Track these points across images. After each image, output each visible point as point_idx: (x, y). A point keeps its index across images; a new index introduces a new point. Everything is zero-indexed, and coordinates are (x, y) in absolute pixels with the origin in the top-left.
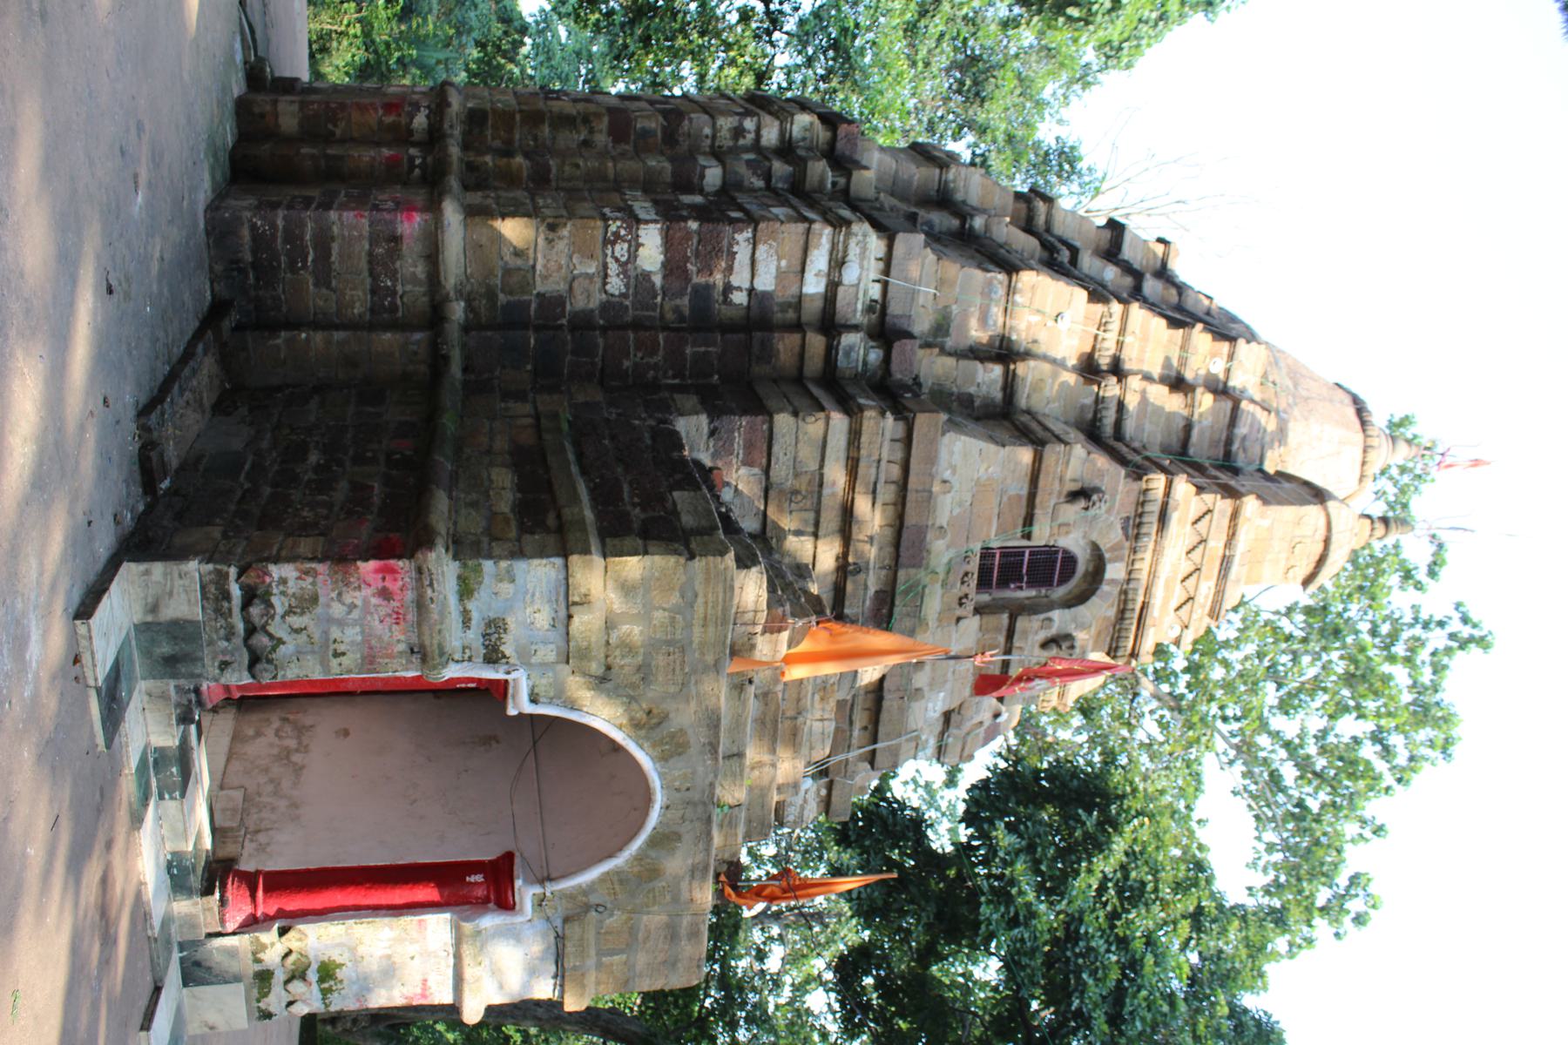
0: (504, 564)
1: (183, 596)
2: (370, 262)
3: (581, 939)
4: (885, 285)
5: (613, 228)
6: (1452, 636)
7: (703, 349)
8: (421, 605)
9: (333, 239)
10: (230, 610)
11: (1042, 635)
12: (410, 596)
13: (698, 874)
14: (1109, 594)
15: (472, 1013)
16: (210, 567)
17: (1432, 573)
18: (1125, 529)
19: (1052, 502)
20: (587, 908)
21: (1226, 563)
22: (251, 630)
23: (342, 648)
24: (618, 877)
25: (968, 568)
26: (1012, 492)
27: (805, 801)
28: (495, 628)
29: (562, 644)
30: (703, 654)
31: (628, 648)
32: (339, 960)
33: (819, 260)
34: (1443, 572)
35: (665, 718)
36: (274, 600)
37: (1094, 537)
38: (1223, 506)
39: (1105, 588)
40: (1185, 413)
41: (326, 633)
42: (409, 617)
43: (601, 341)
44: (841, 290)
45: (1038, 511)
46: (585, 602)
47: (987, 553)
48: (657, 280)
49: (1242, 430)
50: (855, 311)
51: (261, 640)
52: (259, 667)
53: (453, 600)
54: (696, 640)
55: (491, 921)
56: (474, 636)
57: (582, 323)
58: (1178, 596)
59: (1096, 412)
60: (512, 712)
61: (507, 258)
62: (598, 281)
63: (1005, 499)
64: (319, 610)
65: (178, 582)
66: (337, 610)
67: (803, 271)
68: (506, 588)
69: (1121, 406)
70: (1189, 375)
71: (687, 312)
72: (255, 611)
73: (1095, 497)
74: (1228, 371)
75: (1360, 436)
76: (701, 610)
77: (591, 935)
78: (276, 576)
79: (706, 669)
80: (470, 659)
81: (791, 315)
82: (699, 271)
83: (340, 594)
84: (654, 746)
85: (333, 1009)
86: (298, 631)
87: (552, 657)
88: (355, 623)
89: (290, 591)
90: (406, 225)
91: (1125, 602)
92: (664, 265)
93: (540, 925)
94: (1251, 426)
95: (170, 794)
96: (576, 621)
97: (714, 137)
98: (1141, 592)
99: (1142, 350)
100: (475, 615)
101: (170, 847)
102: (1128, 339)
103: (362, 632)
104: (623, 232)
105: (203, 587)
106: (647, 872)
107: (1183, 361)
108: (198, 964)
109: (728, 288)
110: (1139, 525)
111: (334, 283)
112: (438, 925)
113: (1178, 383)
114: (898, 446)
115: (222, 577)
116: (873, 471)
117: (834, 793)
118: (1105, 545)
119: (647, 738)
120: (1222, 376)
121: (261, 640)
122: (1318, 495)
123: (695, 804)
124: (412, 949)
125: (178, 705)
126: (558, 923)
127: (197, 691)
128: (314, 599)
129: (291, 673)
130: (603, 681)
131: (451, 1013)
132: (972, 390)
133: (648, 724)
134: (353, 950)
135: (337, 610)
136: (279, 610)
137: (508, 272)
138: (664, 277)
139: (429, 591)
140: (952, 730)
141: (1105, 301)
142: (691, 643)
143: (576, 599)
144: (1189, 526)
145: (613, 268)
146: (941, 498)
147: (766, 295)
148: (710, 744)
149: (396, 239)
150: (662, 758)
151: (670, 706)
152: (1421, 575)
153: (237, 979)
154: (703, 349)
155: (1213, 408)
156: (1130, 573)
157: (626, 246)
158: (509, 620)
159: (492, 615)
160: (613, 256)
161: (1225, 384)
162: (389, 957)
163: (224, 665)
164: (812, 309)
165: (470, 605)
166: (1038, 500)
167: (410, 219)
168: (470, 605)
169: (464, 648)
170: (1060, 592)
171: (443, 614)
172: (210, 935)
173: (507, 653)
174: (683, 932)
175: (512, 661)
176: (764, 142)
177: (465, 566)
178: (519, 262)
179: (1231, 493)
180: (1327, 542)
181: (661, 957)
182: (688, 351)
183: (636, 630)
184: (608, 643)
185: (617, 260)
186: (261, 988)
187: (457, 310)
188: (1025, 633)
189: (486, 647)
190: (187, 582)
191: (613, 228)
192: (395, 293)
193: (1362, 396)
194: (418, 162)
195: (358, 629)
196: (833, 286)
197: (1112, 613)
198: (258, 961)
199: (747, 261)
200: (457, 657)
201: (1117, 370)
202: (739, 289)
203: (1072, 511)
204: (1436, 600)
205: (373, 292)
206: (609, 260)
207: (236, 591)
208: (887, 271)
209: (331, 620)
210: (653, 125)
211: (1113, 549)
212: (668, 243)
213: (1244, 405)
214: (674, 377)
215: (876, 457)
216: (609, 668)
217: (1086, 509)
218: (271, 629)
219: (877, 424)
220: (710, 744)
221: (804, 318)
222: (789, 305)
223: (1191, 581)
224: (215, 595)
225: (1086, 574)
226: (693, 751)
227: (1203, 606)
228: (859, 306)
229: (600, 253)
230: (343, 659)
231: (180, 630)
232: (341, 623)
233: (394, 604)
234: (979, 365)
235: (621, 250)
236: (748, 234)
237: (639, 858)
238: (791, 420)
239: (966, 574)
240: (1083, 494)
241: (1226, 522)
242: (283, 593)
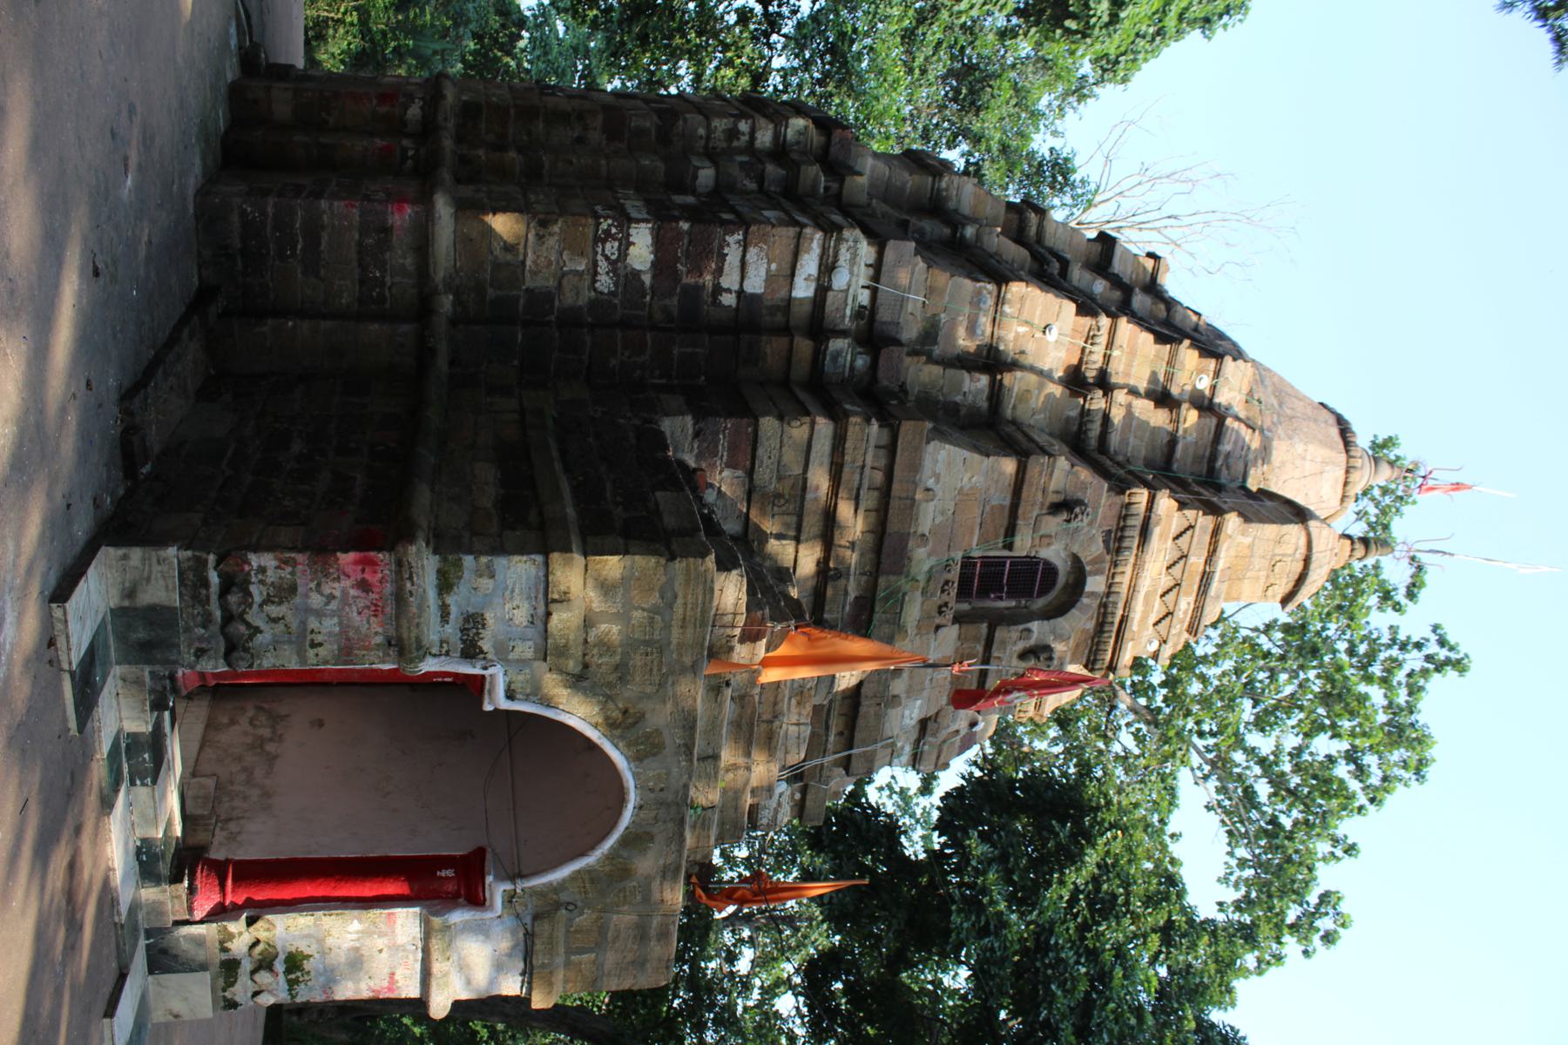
0: (484, 559)
1: (161, 582)
2: (359, 252)
3: (551, 937)
4: (874, 292)
5: (604, 226)
6: (1429, 658)
7: (690, 350)
8: (400, 598)
9: (323, 227)
10: (208, 597)
11: (1021, 646)
12: (388, 588)
13: (669, 874)
14: (1088, 606)
15: (439, 1007)
16: (189, 553)
17: (1411, 595)
18: (1106, 542)
20: (558, 905)
21: (1206, 579)
22: (228, 618)
23: (319, 638)
24: (588, 875)
25: (949, 576)
27: (779, 804)
28: (473, 622)
29: (540, 641)
30: (680, 655)
31: (605, 646)
32: (307, 951)
33: (809, 265)
34: (1423, 594)
35: (641, 717)
36: (253, 588)
37: (1075, 549)
38: (1205, 522)
39: (1085, 600)
40: (1170, 428)
41: (303, 623)
42: (388, 609)
43: (588, 339)
44: (830, 294)
45: (1020, 522)
46: (564, 599)
47: (968, 563)
48: (647, 279)
49: (1226, 447)
50: (844, 316)
52: (235, 655)
53: (432, 594)
54: (674, 641)
55: (458, 917)
56: (451, 630)
57: (571, 320)
58: (1157, 610)
59: (1081, 425)
60: (488, 707)
61: (497, 252)
62: (587, 278)
63: (988, 508)
64: (298, 600)
65: (156, 568)
66: (316, 600)
67: (793, 275)
68: (486, 584)
69: (1106, 418)
70: (1175, 391)
71: (675, 314)
72: (233, 599)
73: (1077, 510)
74: (1214, 388)
75: (1344, 455)
76: (681, 611)
77: (560, 934)
78: (255, 565)
79: (683, 671)
80: (447, 654)
81: (779, 318)
82: (689, 272)
83: (319, 585)
84: (629, 745)
85: (299, 1000)
86: (275, 620)
87: (529, 654)
88: (333, 614)
89: (269, 580)
90: (397, 217)
91: (1105, 614)
92: (654, 264)
93: (509, 921)
94: (1236, 443)
95: (142, 780)
96: (555, 619)
97: (708, 138)
98: (1121, 605)
99: (1129, 365)
100: (454, 610)
101: (140, 833)
102: (1116, 353)
103: (340, 624)
104: (614, 230)
105: (181, 574)
106: (617, 872)
107: (1170, 377)
108: (164, 952)
109: (718, 290)
110: (1121, 539)
111: (322, 272)
112: (406, 922)
113: (1162, 398)
114: (882, 452)
115: (201, 565)
116: (857, 477)
117: (809, 797)
118: (1086, 557)
119: (622, 737)
120: (1207, 392)
122: (1299, 514)
123: (668, 805)
124: (380, 942)
125: (152, 691)
126: (528, 920)
127: (172, 677)
128: (293, 589)
129: (268, 662)
130: (580, 680)
131: (418, 1007)
132: (958, 398)
133: (622, 724)
134: (321, 941)
136: (257, 599)
137: (497, 266)
138: (654, 277)
139: (408, 585)
140: (929, 739)
141: (1094, 315)
142: (669, 643)
143: (556, 596)
145: (603, 266)
146: (924, 505)
147: (753, 296)
148: (686, 745)
149: (386, 230)
150: (637, 758)
151: (646, 706)
152: (1400, 596)
153: (203, 967)
154: (690, 350)
155: (1198, 423)
156: (1110, 586)
157: (616, 244)
158: (489, 616)
159: (471, 610)
160: (604, 254)
161: (1211, 400)
162: (357, 949)
163: (200, 653)
164: (801, 313)
165: (450, 600)
166: (1020, 511)
167: (400, 210)
168: (450, 600)
169: (442, 642)
170: (1040, 603)
171: (422, 607)
172: (178, 923)
173: (485, 648)
174: (653, 932)
175: (489, 656)
176: (758, 144)
177: (444, 560)
178: (509, 257)
179: (1215, 510)
180: (1307, 561)
181: (630, 957)
182: (676, 351)
183: (615, 629)
184: (586, 641)
185: (607, 258)
186: (226, 978)
187: (446, 303)
188: (1003, 643)
189: (464, 642)
190: (165, 568)
191: (604, 226)
192: (383, 284)
193: (1347, 416)
194: (410, 153)
195: (336, 620)
197: (1091, 625)
198: (225, 950)
199: (737, 263)
200: (434, 651)
201: (1104, 383)
202: (729, 291)
203: (1053, 524)
204: (1414, 623)
205: (362, 282)
206: (599, 257)
207: (214, 578)
208: (876, 277)
209: (308, 610)
210: (648, 124)
211: (1094, 561)
212: (659, 243)
213: (1229, 421)
214: (660, 377)
215: (860, 463)
216: (586, 666)
217: (1068, 521)
218: (248, 618)
219: (863, 430)
220: (686, 745)
221: (792, 323)
222: (778, 308)
223: (1171, 596)
224: (193, 581)
225: (1067, 585)
226: (669, 751)
227: (1182, 622)
228: (848, 312)
229: (589, 250)
230: (321, 650)
231: (158, 616)
232: (319, 614)
233: (372, 596)
234: (966, 375)
235: (611, 248)
236: (739, 236)
237: (611, 857)
238: (776, 423)
239: (947, 582)
240: (1066, 506)
241: (1208, 538)
242: (262, 582)
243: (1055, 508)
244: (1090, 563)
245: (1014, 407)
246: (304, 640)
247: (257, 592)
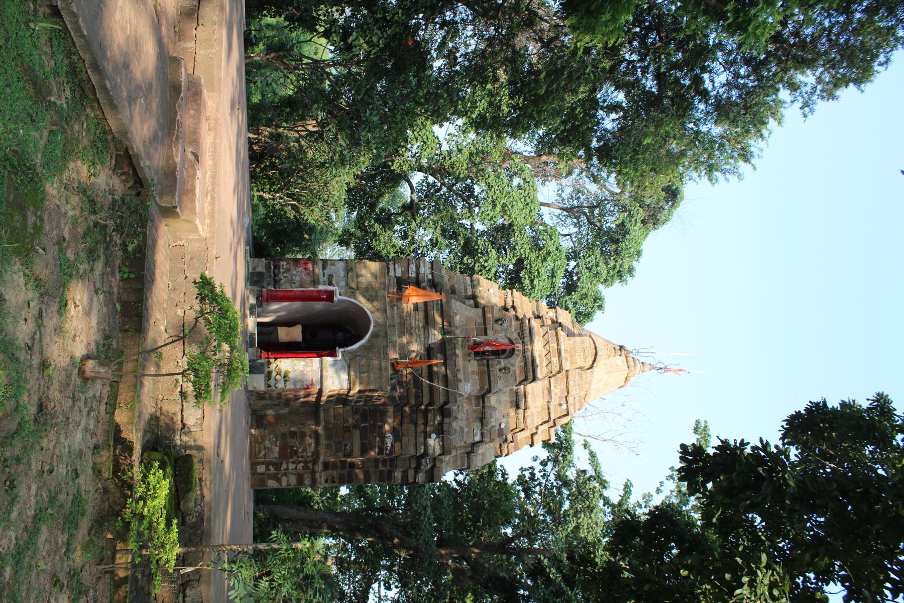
4: (432, 274)
11: (498, 367)
22: (275, 275)
24: (363, 347)
28: (331, 276)
33: (413, 268)
51: (277, 278)
56: (326, 279)
58: (545, 363)
66: (295, 272)
107: (538, 311)
118: (513, 338)
121: (277, 278)
124: (309, 369)
129: (283, 288)
135: (295, 272)
180: (596, 348)
181: (377, 376)
196: (418, 274)
197: (522, 364)
201: (514, 307)
203: (497, 326)
223: (548, 356)
224: (268, 267)
231: (260, 275)
237: (369, 340)
243: (497, 321)
246: (292, 282)
247: (282, 271)
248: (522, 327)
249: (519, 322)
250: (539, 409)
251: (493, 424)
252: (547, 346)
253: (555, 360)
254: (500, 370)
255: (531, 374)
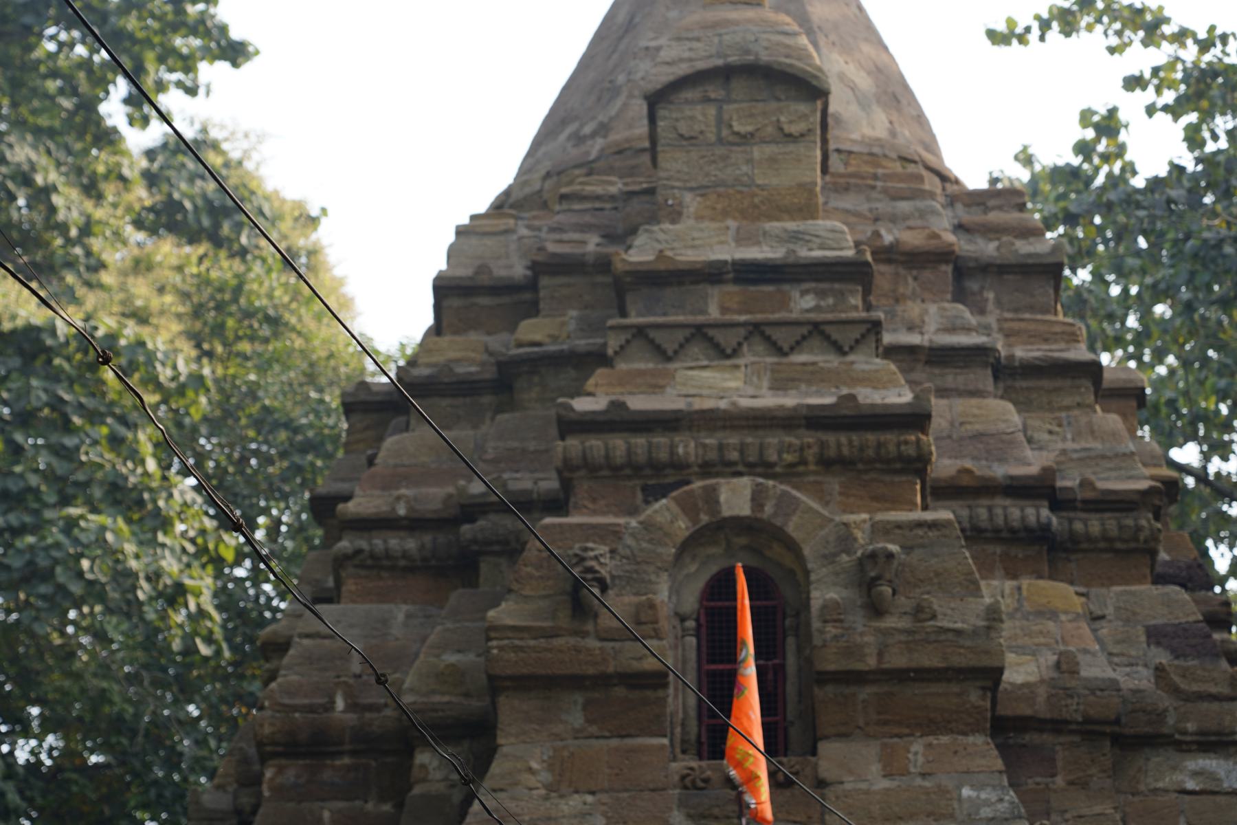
11: (858, 620)
19: (592, 643)
21: (750, 273)
26: (577, 718)
63: (593, 729)
110: (657, 467)
118: (683, 527)
144: (672, 366)
166: (591, 671)
211: (689, 508)
223: (782, 337)
234: (417, 790)
244: (695, 520)
245: (467, 695)
248: (612, 472)
249: (583, 488)
250: (1040, 425)
251: (1143, 679)
252: (727, 339)
253: (803, 303)
254: (876, 609)
255: (890, 438)
